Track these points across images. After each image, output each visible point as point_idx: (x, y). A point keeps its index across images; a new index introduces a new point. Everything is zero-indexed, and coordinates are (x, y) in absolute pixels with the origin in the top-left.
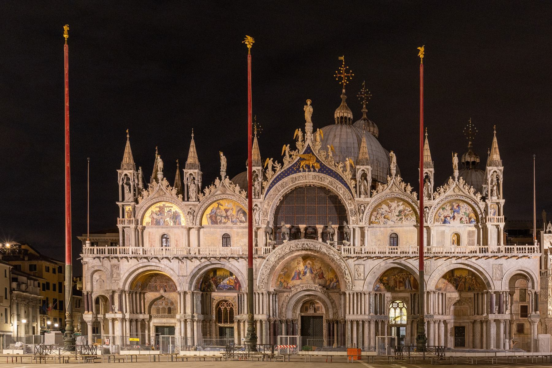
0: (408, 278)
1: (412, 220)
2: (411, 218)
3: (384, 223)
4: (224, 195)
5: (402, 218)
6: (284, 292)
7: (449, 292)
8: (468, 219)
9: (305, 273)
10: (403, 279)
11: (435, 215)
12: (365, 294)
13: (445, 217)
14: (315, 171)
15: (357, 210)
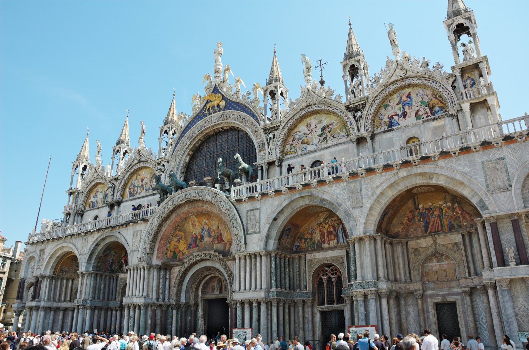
0: (341, 226)
1: (341, 135)
2: (339, 134)
3: (302, 151)
4: (140, 164)
5: (327, 137)
6: (176, 265)
7: (414, 238)
8: (428, 110)
9: (202, 237)
10: (334, 227)
11: (373, 120)
12: (261, 256)
13: (391, 118)
14: (220, 110)
15: (265, 141)
